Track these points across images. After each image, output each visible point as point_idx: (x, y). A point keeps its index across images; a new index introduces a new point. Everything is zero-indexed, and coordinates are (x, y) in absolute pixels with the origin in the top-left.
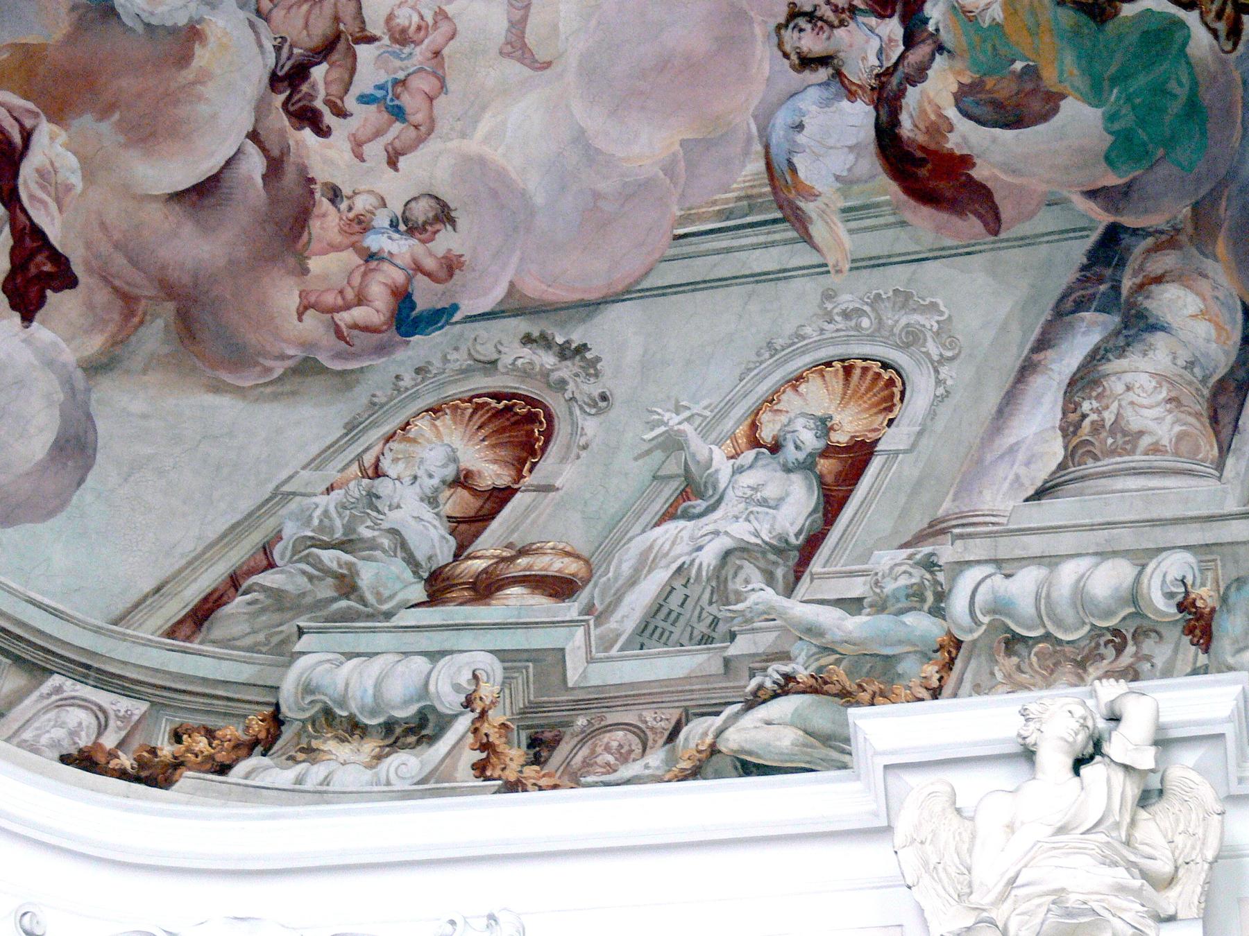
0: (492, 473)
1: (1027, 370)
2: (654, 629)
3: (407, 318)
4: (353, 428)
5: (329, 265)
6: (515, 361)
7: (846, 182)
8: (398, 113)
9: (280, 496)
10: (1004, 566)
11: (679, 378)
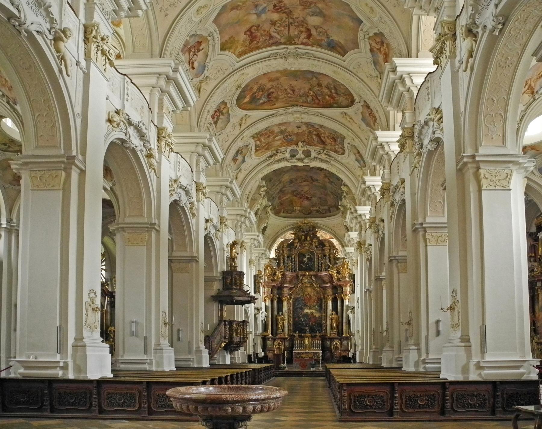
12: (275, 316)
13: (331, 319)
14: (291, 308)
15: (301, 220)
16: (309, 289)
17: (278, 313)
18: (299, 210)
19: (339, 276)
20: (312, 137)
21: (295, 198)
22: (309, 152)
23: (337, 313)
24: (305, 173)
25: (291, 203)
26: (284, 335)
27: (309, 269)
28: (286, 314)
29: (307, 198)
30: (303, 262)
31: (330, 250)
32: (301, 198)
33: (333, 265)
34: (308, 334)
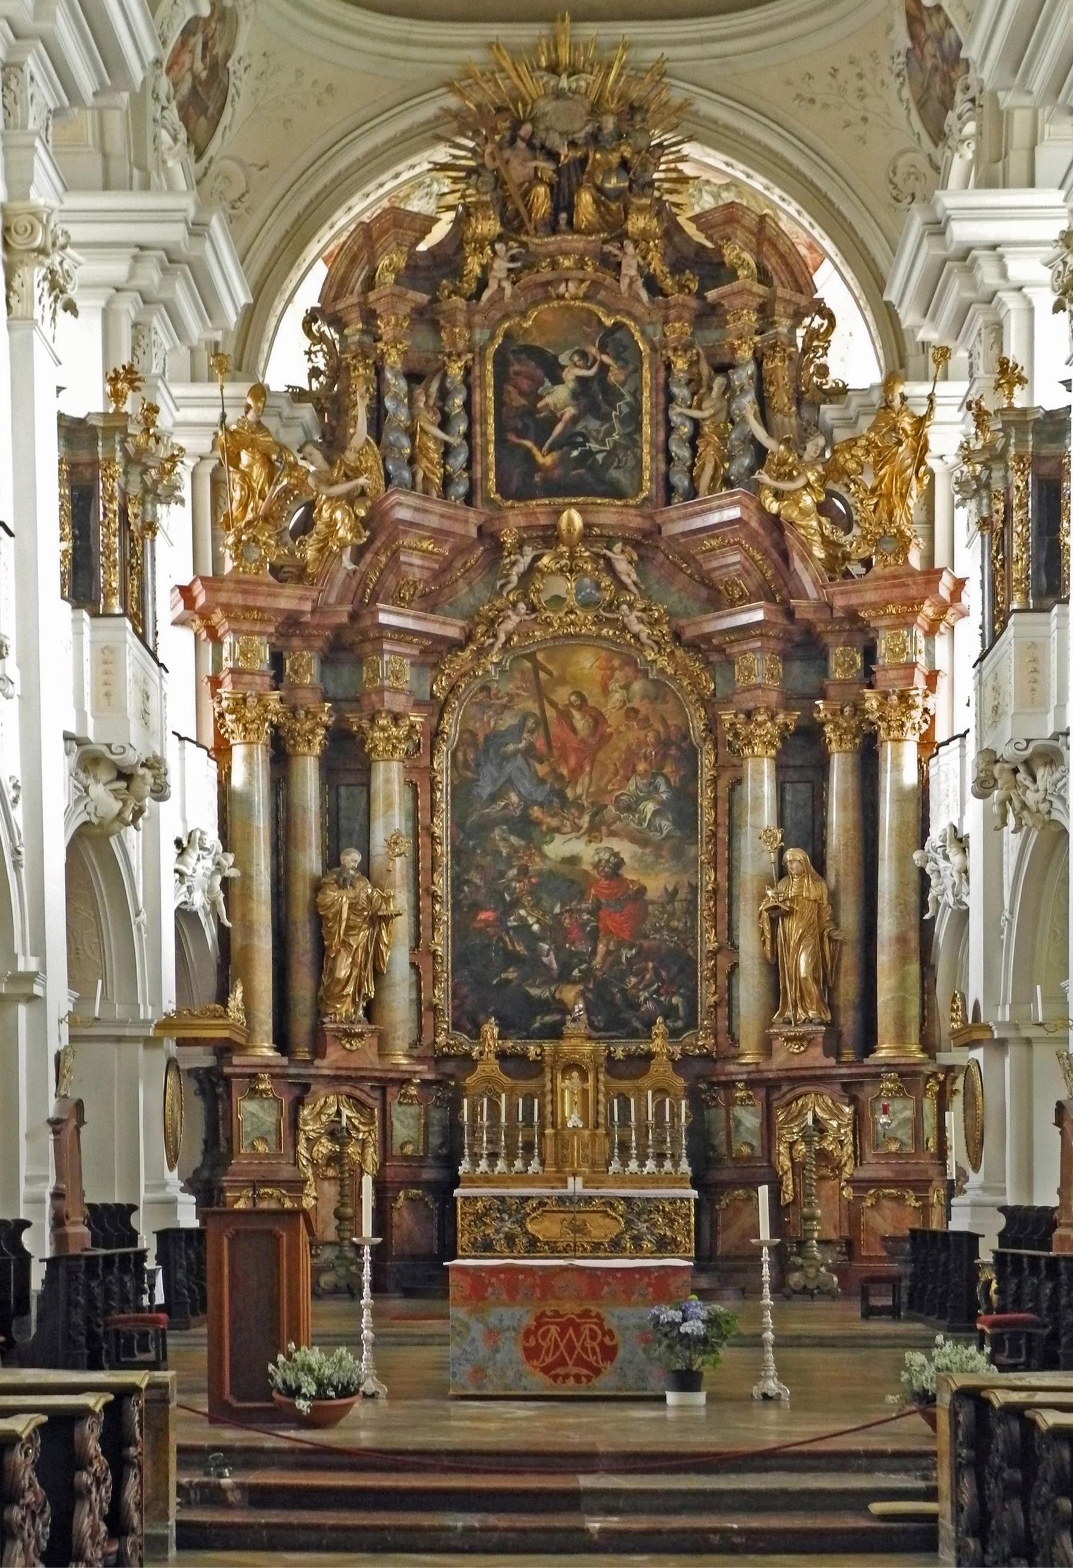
12: (301, 892)
13: (776, 915)
14: (442, 826)
16: (587, 662)
17: (332, 860)
19: (840, 536)
23: (819, 864)
26: (383, 1051)
27: (590, 481)
28: (400, 867)
30: (541, 426)
31: (765, 311)
33: (797, 444)
34: (579, 1045)
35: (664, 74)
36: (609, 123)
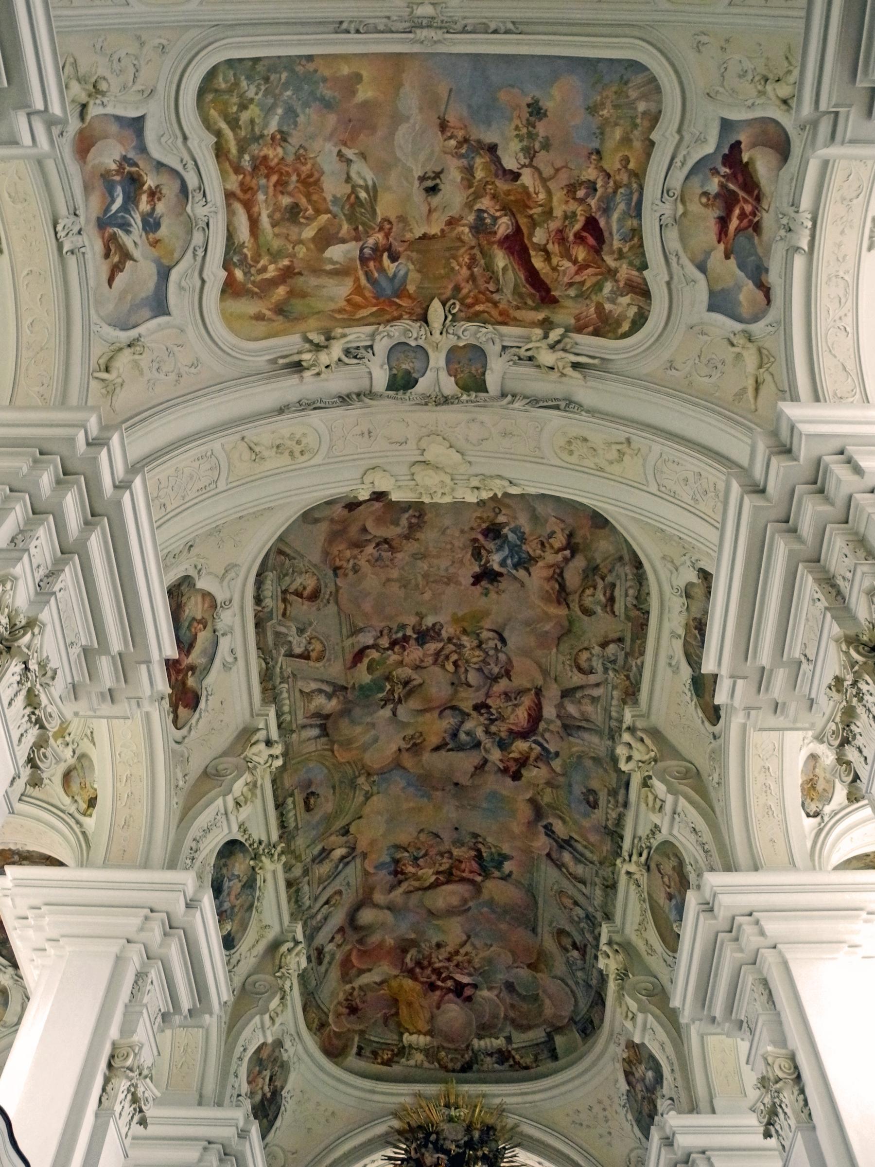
0: (305, 594)
1: (322, 681)
2: (277, 634)
3: (336, 570)
4: (315, 566)
5: (348, 553)
6: (326, 593)
7: (358, 642)
8: (377, 560)
9: (302, 556)
10: (288, 691)
11: (324, 620)
15: (431, 1089)
18: (430, 1053)
20: (489, 268)
21: (408, 983)
22: (477, 353)
24: (451, 812)
25: (393, 1010)
29: (459, 989)
32: (432, 987)
35: (503, 1111)
36: (476, 1135)
